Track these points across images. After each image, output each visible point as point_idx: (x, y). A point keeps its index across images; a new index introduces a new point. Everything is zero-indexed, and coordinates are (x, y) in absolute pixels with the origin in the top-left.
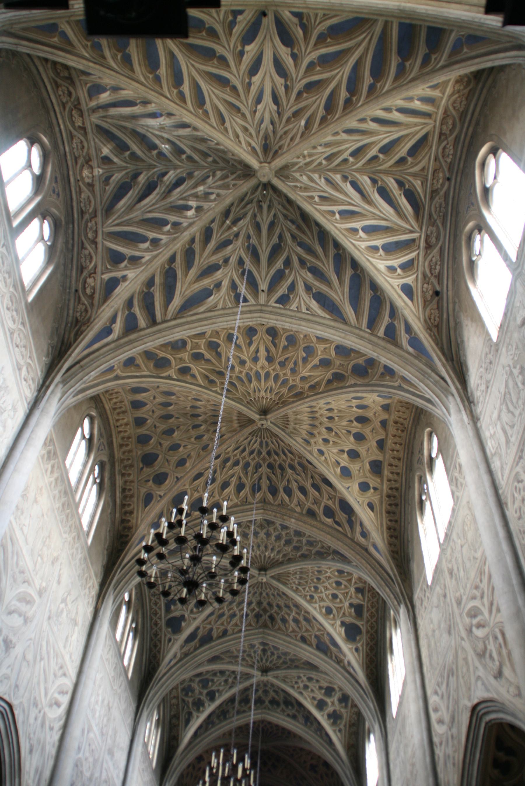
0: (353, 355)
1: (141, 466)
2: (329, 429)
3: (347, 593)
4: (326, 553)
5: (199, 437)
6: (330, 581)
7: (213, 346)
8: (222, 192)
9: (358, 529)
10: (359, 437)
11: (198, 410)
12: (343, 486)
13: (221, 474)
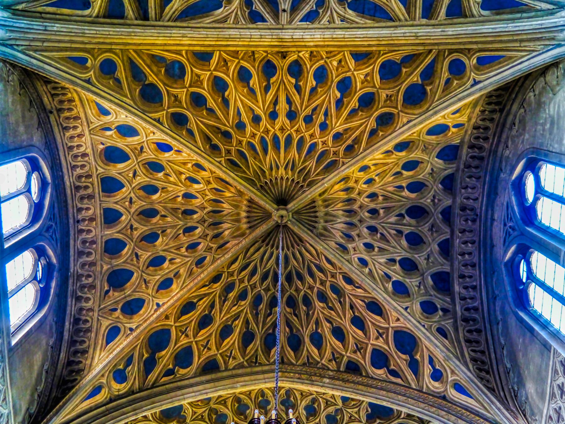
1: (106, 288)
2: (373, 230)
5: (193, 247)
9: (427, 370)
11: (194, 201)
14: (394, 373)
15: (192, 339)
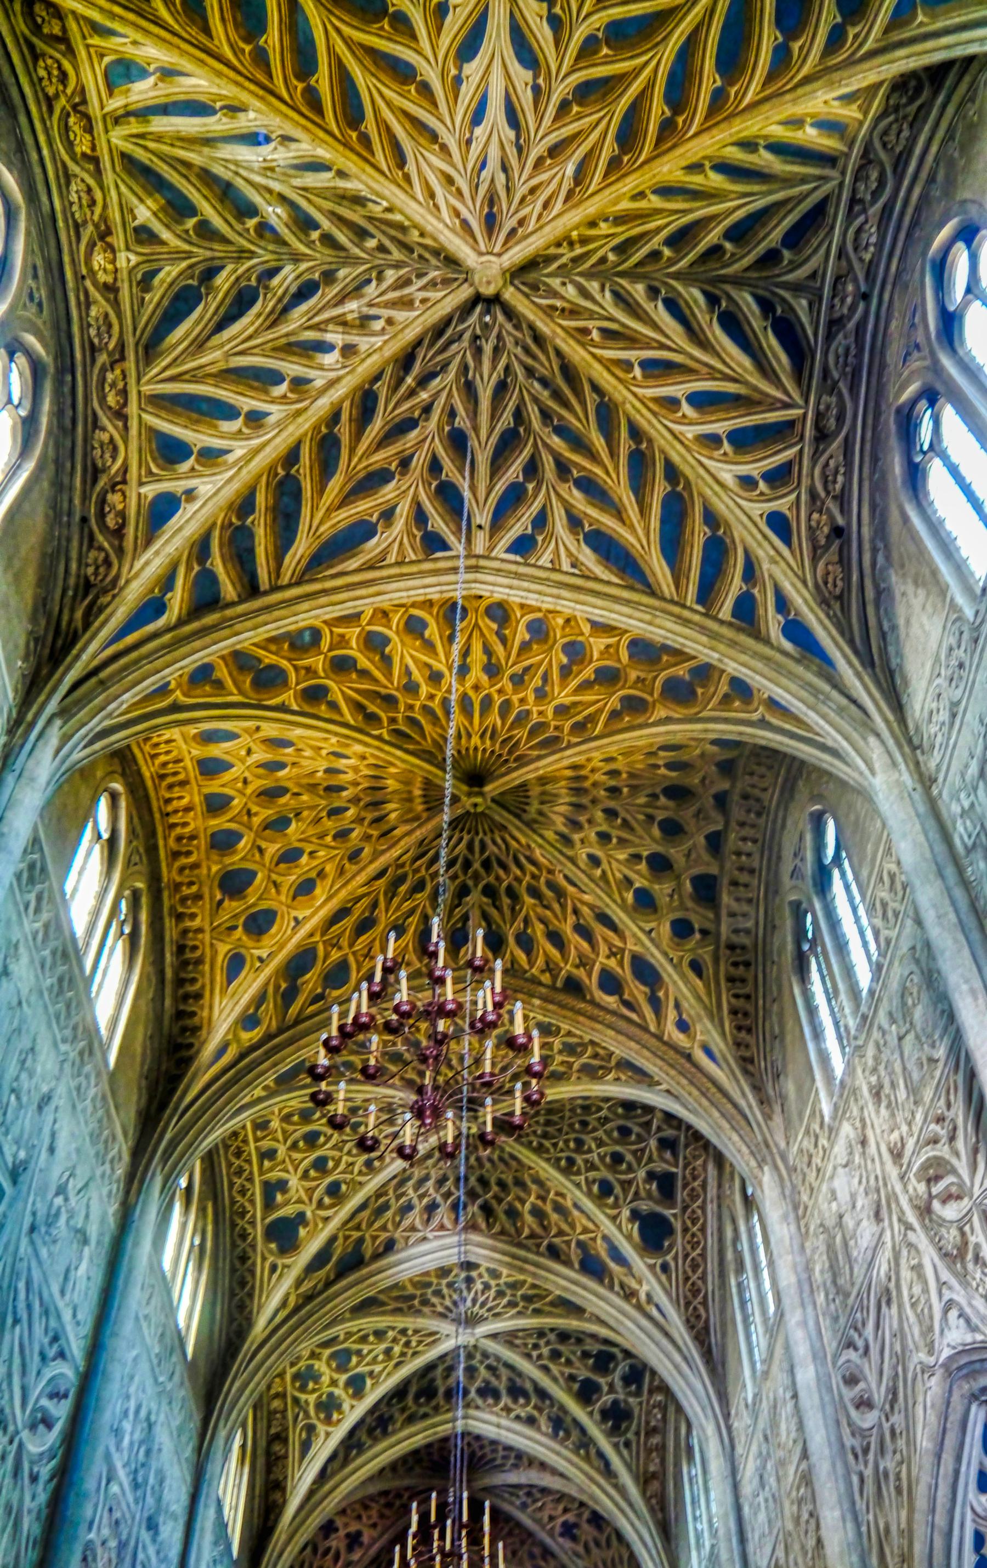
0: (665, 658)
2: (611, 813)
3: (643, 1150)
4: (601, 1067)
5: (342, 835)
6: (608, 1126)
7: (374, 643)
8: (401, 316)
9: (672, 1015)
10: (672, 829)
11: (342, 776)
12: (641, 929)
13: (387, 910)
14: (628, 1005)
15: (347, 950)
